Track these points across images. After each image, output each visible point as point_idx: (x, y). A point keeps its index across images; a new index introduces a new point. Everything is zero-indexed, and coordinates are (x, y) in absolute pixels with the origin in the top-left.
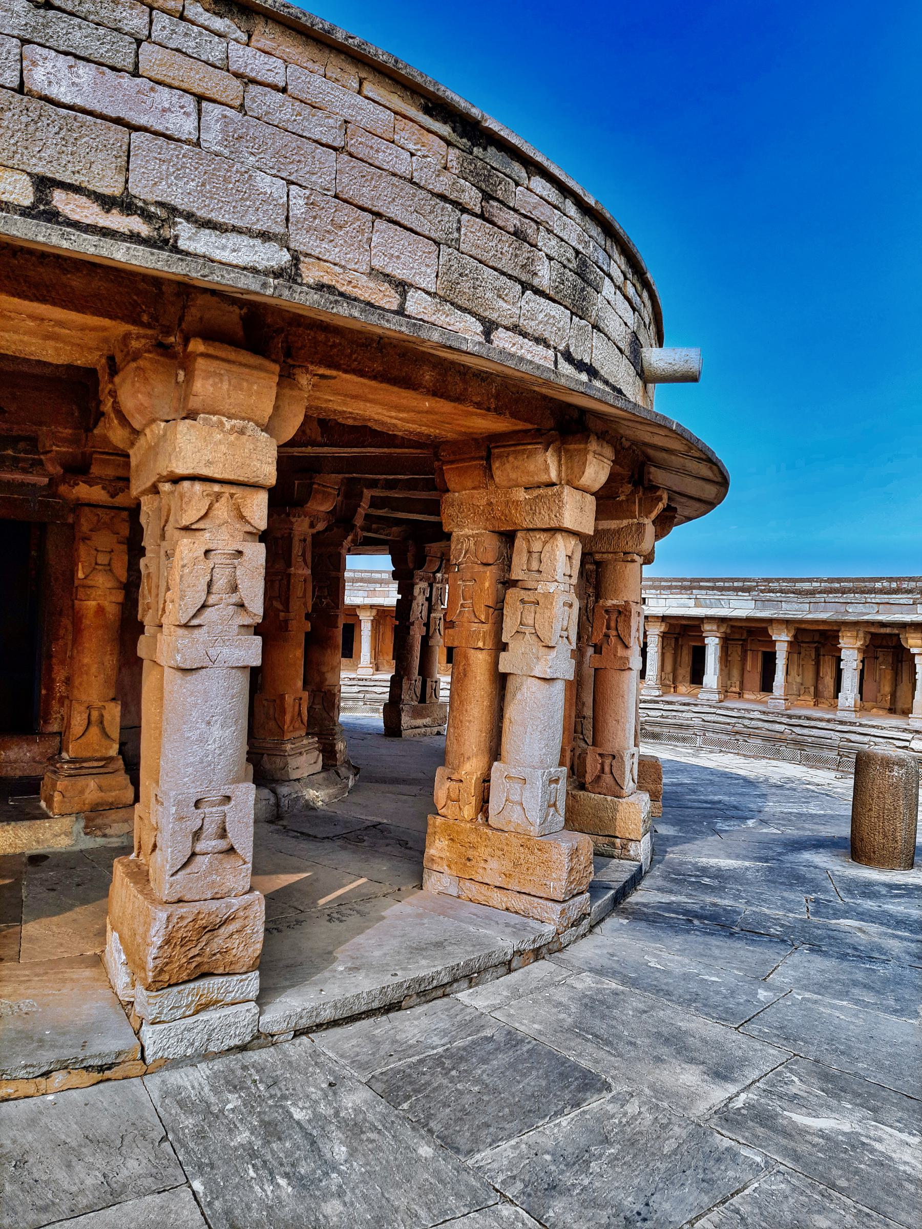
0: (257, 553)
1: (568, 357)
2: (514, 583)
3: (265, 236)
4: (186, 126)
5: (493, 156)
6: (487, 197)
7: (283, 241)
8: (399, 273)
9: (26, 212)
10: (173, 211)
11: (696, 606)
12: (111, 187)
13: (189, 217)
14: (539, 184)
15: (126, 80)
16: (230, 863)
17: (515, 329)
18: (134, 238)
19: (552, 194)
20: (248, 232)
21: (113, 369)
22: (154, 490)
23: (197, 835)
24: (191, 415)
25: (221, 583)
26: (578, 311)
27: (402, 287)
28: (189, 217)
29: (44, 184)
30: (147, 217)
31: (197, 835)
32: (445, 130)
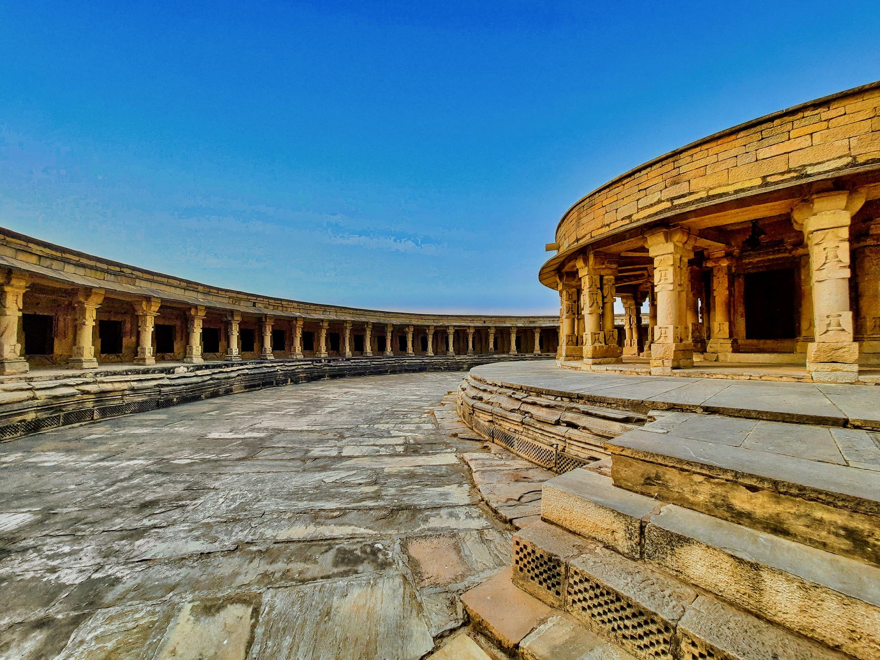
7: (849, 155)
9: (760, 186)
12: (785, 169)
16: (842, 333)
18: (793, 178)
20: (834, 159)
21: (792, 210)
22: (809, 238)
23: (829, 325)
24: (815, 214)
28: (810, 165)
29: (764, 178)
30: (795, 171)
31: (829, 325)
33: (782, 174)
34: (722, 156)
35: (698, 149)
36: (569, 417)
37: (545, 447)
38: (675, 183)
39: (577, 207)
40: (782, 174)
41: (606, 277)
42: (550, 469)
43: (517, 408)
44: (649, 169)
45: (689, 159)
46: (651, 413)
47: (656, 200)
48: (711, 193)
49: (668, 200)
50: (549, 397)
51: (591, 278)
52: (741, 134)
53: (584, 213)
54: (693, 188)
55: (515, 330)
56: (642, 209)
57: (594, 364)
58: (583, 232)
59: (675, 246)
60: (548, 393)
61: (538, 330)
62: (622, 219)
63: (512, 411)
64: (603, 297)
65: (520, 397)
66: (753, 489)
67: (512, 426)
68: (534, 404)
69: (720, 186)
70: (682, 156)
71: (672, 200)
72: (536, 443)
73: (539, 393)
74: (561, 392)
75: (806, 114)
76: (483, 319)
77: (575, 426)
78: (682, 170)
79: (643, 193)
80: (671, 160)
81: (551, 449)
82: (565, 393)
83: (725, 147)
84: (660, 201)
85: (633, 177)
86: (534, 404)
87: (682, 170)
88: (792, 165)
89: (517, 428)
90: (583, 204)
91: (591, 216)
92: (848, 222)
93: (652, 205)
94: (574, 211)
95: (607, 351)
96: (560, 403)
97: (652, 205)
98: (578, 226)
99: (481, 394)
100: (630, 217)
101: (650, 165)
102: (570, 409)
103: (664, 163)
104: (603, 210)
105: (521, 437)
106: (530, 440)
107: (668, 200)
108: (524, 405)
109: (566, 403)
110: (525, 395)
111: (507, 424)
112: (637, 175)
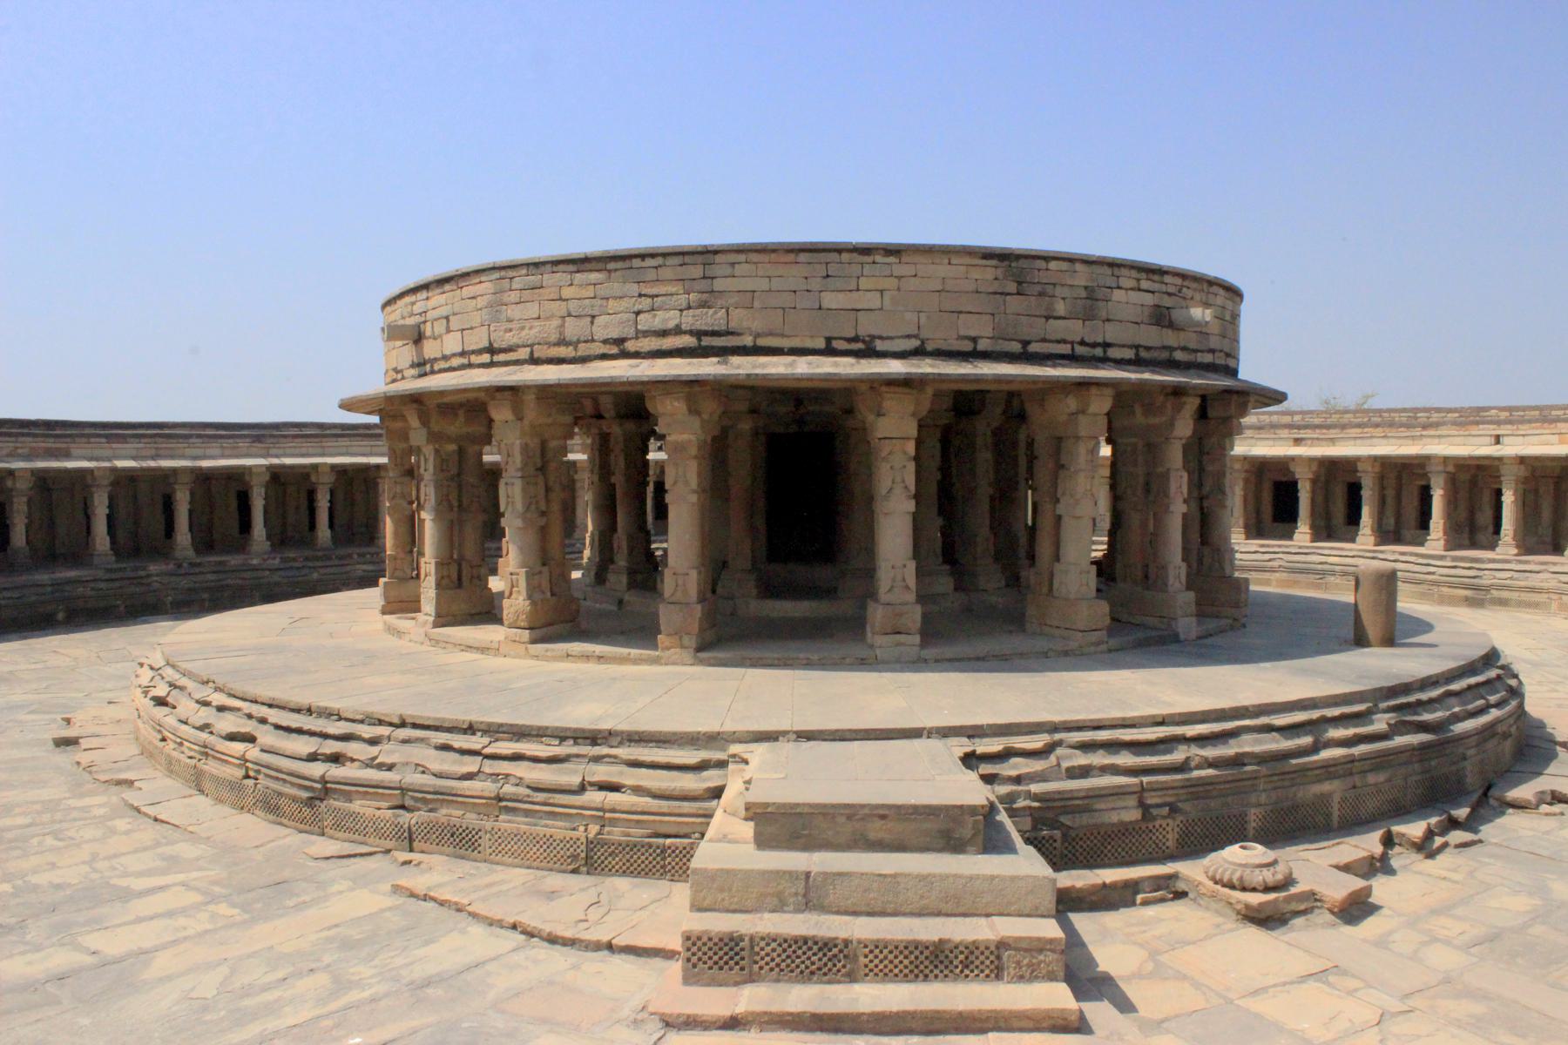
0: (912, 467)
1: (1082, 343)
2: (1063, 466)
3: (908, 337)
4: (877, 304)
5: (1023, 263)
6: (1020, 283)
7: (916, 336)
8: (973, 333)
10: (873, 337)
11: (1561, 442)
12: (852, 335)
13: (881, 338)
14: (1053, 265)
15: (855, 294)
17: (1044, 340)
19: (1064, 266)
25: (898, 479)
26: (1088, 316)
27: (974, 340)
28: (881, 338)
30: (864, 341)
32: (994, 262)
33: (849, 340)
34: (776, 284)
35: (742, 257)
36: (602, 773)
38: (703, 305)
39: (496, 275)
40: (849, 340)
43: (474, 769)
44: (659, 261)
45: (728, 271)
46: (735, 749)
47: (671, 325)
48: (762, 342)
49: (691, 333)
51: (525, 448)
52: (803, 257)
53: (513, 296)
54: (733, 325)
56: (646, 334)
57: (534, 641)
59: (703, 421)
62: (605, 342)
63: (469, 777)
65: (477, 747)
66: (883, 817)
68: (517, 757)
69: (771, 334)
70: (718, 258)
71: (699, 334)
73: (520, 733)
74: (576, 730)
75: (879, 258)
77: (614, 788)
78: (719, 285)
79: (645, 303)
80: (700, 259)
82: (583, 730)
83: (780, 270)
84: (678, 331)
85: (627, 264)
86: (517, 757)
87: (719, 285)
88: (862, 332)
90: (511, 273)
91: (532, 310)
92: (914, 433)
93: (664, 333)
97: (664, 333)
100: (620, 341)
101: (665, 255)
102: (597, 759)
103: (687, 259)
107: (691, 333)
110: (486, 740)
112: (636, 263)
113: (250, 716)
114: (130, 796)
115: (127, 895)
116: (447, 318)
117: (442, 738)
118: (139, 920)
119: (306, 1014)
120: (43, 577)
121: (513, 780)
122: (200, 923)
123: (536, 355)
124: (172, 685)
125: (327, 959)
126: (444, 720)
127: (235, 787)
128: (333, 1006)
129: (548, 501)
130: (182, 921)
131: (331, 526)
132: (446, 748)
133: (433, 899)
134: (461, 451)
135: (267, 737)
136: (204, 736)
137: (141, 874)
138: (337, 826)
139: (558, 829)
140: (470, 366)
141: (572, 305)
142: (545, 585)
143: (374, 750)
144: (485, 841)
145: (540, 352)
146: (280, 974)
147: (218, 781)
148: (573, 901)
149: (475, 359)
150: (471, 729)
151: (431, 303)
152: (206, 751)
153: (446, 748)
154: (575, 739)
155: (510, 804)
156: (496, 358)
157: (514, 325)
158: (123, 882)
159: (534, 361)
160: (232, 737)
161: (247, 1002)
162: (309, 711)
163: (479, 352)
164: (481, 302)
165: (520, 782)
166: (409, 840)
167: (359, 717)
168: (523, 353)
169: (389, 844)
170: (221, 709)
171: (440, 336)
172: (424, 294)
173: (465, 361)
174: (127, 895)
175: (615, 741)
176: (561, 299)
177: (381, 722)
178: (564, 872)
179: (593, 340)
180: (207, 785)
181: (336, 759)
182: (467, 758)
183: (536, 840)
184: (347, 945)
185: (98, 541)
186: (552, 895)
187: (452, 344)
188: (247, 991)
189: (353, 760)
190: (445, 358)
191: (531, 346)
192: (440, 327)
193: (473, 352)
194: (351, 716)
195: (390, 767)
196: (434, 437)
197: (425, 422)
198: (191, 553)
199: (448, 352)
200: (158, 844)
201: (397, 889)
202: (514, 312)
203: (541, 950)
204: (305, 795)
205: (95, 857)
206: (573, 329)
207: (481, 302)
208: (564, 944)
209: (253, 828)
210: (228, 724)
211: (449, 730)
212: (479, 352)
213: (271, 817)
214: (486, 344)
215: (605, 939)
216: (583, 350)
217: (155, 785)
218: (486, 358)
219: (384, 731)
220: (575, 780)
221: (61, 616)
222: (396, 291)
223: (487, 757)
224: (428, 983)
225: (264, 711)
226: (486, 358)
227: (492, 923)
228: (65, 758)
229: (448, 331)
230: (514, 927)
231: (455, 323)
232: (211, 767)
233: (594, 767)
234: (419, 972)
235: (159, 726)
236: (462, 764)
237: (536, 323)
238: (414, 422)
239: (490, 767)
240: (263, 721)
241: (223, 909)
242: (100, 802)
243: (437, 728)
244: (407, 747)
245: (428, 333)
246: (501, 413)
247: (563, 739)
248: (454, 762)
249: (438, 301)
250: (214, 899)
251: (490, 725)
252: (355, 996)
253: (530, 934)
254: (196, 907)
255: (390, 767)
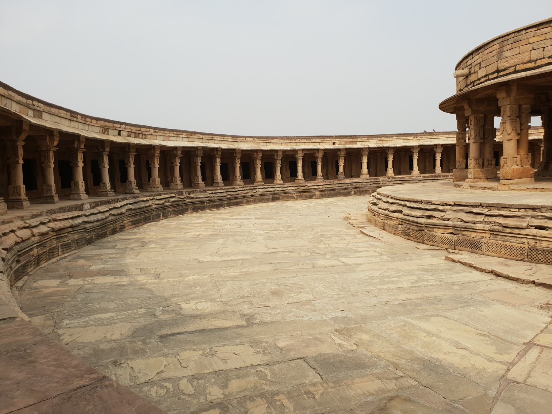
36: (537, 222)
37: (516, 245)
41: (524, 106)
42: (521, 260)
50: (512, 210)
51: (511, 109)
53: (509, 47)
55: (366, 152)
58: (506, 65)
60: (510, 207)
61: (392, 151)
64: (521, 124)
67: (478, 234)
72: (507, 244)
74: (525, 205)
76: (333, 140)
81: (522, 246)
82: (528, 205)
89: (483, 235)
90: (507, 38)
91: (517, 51)
94: (495, 43)
95: (522, 172)
96: (525, 214)
98: (500, 58)
99: (428, 213)
104: (530, 47)
105: (489, 241)
106: (500, 242)
108: (487, 218)
109: (531, 213)
110: (487, 210)
111: (472, 233)
113: (401, 205)
114: (362, 230)
115: (356, 251)
116: (480, 63)
117: (469, 209)
118: (358, 257)
119: (406, 285)
120: (348, 181)
121: (497, 224)
122: (378, 259)
123: (517, 69)
124: (378, 199)
125: (417, 273)
126: (469, 203)
127: (396, 227)
128: (416, 285)
129: (521, 130)
130: (371, 259)
131: (441, 166)
132: (471, 212)
133: (460, 262)
134: (485, 116)
135: (406, 211)
136: (386, 212)
137: (360, 248)
138: (428, 240)
139: (515, 243)
140: (489, 80)
141: (535, 46)
142: (519, 163)
143: (443, 214)
144: (484, 246)
145: (518, 68)
146: (400, 274)
147: (389, 225)
148: (519, 269)
149: (491, 77)
150: (481, 205)
151: (474, 60)
152: (387, 217)
153: (471, 212)
154: (525, 209)
155: (495, 233)
156: (500, 74)
157: (508, 59)
158: (356, 249)
159: (516, 72)
160: (395, 211)
161: (387, 279)
162: (421, 202)
163: (493, 73)
164: (494, 53)
165: (500, 224)
166: (454, 246)
167: (438, 203)
168: (511, 70)
169: (447, 247)
170: (392, 203)
171: (477, 71)
172: (471, 57)
173: (487, 78)
174: (356, 251)
175: (543, 210)
176: (529, 43)
177: (446, 204)
178: (517, 260)
179: (544, 58)
180: (387, 228)
181: (429, 217)
182: (479, 216)
183: (505, 247)
184: (425, 270)
185: (364, 171)
186: (509, 266)
187: (481, 73)
188: (387, 277)
189: (435, 217)
190: (479, 79)
191: (516, 66)
192: (477, 68)
193: (490, 74)
194: (436, 203)
195: (448, 220)
196: (474, 112)
197: (470, 105)
198: (393, 175)
199: (480, 77)
200: (369, 241)
201: (447, 258)
202: (508, 54)
203: (501, 281)
204: (418, 229)
205: (349, 242)
206: (534, 55)
207: (494, 53)
208: (513, 280)
209: (400, 241)
210: (393, 208)
211: (472, 206)
212: (493, 73)
213: (406, 237)
214: (496, 69)
215: (532, 279)
216: (539, 63)
217: (371, 230)
218: (495, 75)
219: (448, 207)
220: (525, 224)
221: (352, 193)
222: (460, 59)
223: (487, 215)
224: (453, 284)
225: (406, 203)
226: (495, 75)
227: (482, 270)
228: (346, 222)
229: (480, 69)
230: (491, 272)
231: (483, 64)
232: (389, 222)
233: (534, 220)
234: (450, 281)
235: (372, 211)
236: (476, 218)
237: (518, 56)
238: (466, 107)
239: (487, 219)
240: (405, 206)
241: (385, 257)
242: (354, 231)
243: (467, 206)
244: (455, 213)
245: (472, 72)
246: (501, 96)
247: (520, 209)
248: (473, 217)
249: (477, 58)
250: (381, 254)
251: (488, 204)
252: (425, 283)
253: (498, 275)
254: (377, 256)
255: (448, 220)
